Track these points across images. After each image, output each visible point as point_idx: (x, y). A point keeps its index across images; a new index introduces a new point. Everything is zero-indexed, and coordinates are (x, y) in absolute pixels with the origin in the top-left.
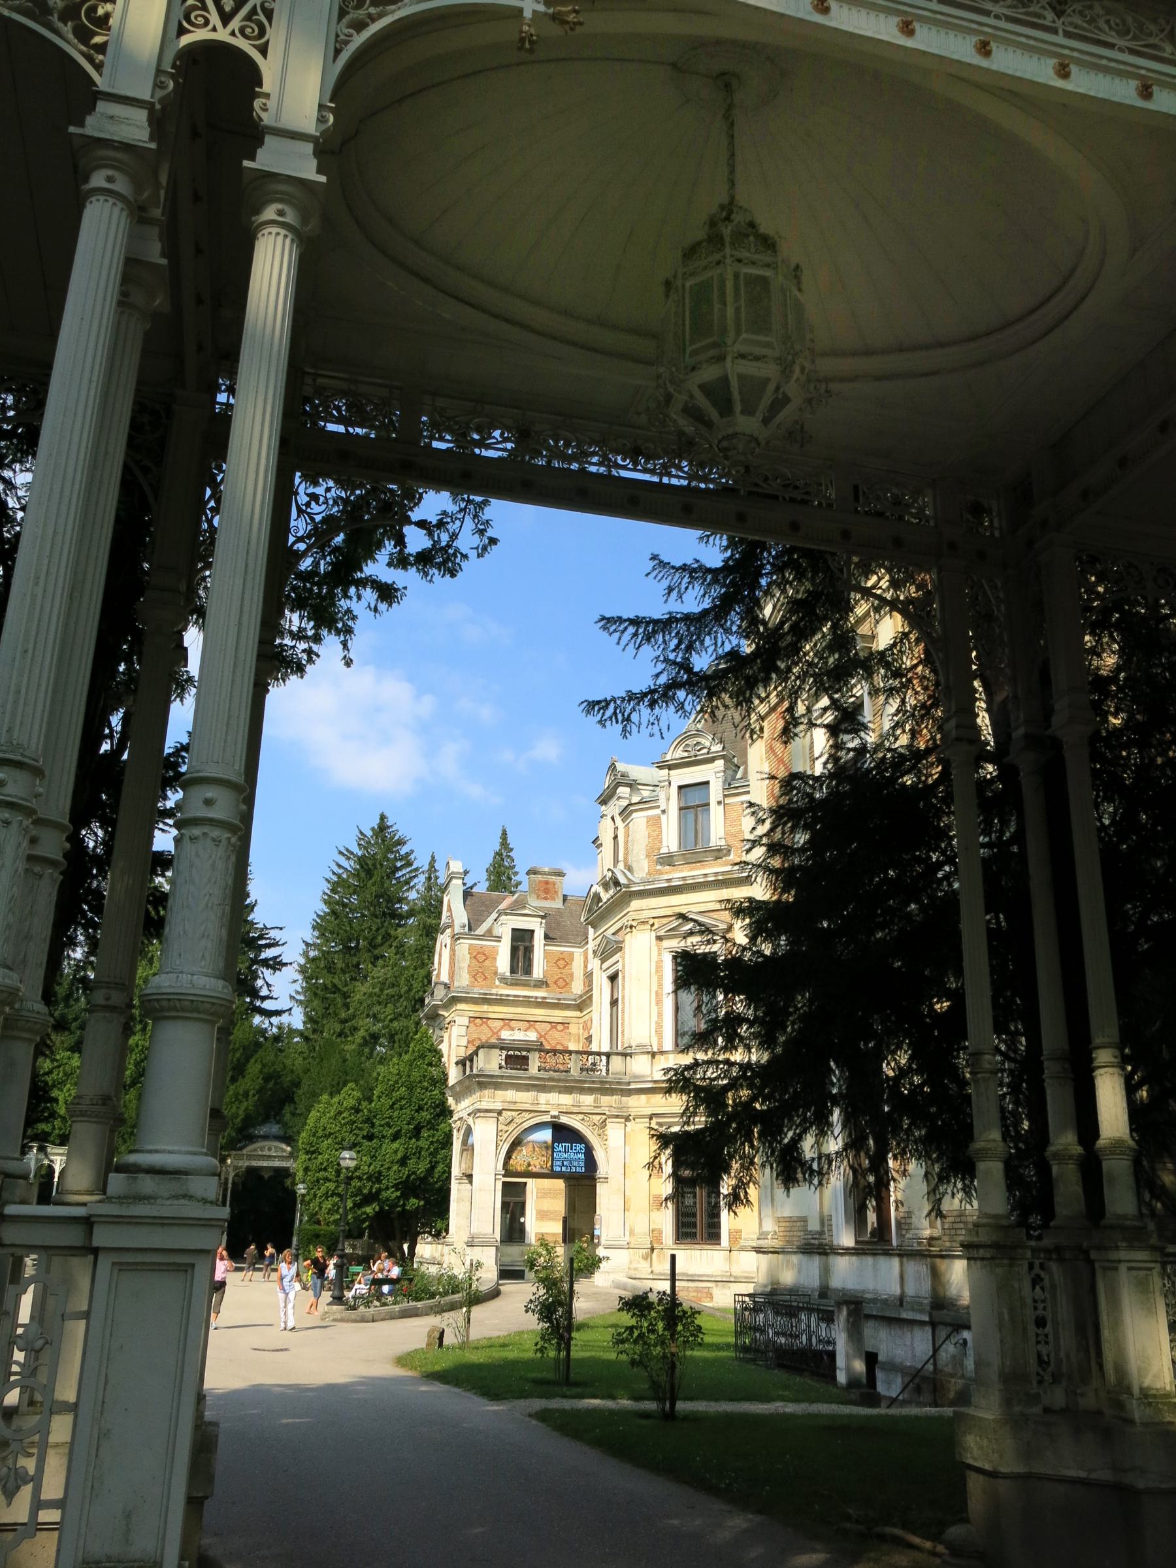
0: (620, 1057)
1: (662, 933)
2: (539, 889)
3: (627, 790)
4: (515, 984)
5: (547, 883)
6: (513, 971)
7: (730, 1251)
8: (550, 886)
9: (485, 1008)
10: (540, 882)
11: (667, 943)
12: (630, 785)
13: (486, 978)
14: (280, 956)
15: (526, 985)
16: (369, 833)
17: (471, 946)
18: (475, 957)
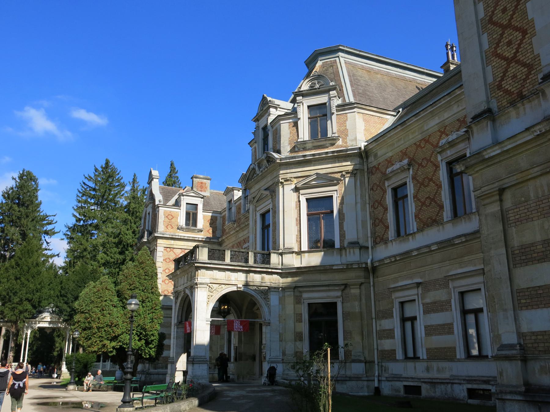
0: (276, 255)
1: (299, 185)
2: (198, 186)
3: (275, 110)
4: (188, 230)
5: (202, 183)
6: (187, 224)
7: (345, 363)
8: (203, 185)
9: (172, 242)
10: (198, 182)
11: (302, 192)
12: (276, 108)
13: (172, 228)
14: (54, 229)
15: (193, 231)
16: (100, 169)
17: (165, 211)
18: (167, 217)
